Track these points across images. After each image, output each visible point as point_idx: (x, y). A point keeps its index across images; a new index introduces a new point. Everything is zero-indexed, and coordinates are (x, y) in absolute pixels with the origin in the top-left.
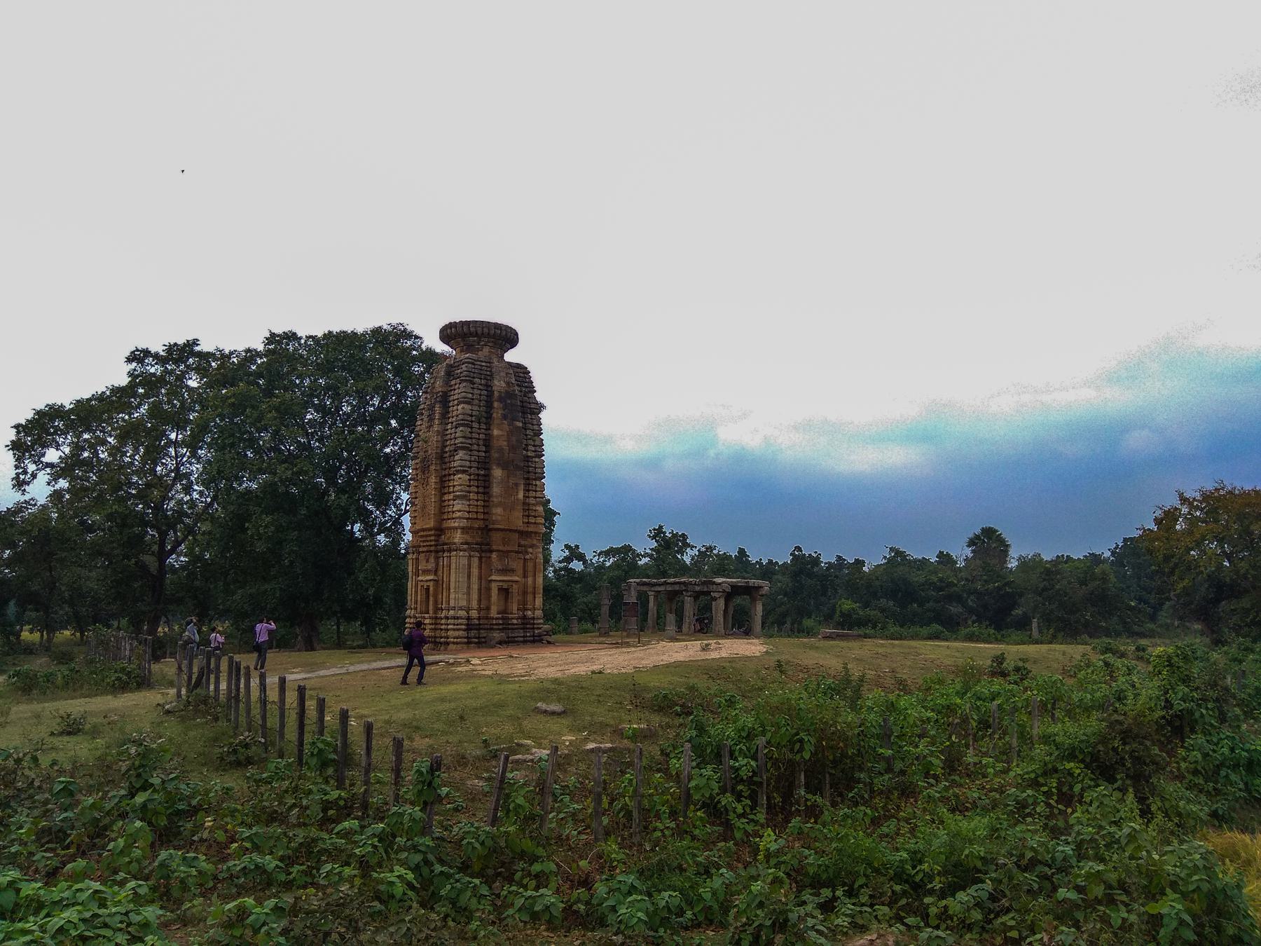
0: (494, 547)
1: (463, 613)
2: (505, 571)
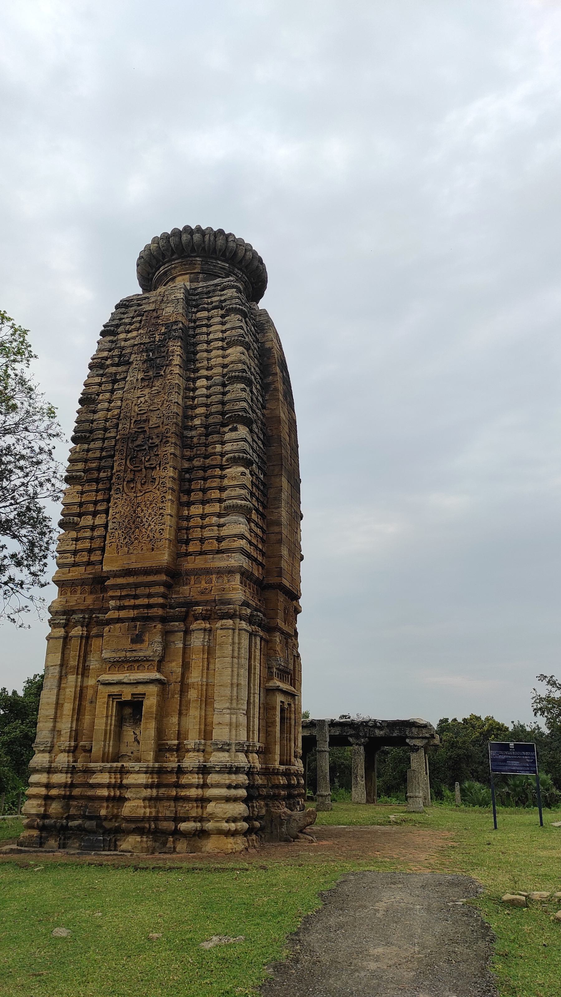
1: (241, 760)
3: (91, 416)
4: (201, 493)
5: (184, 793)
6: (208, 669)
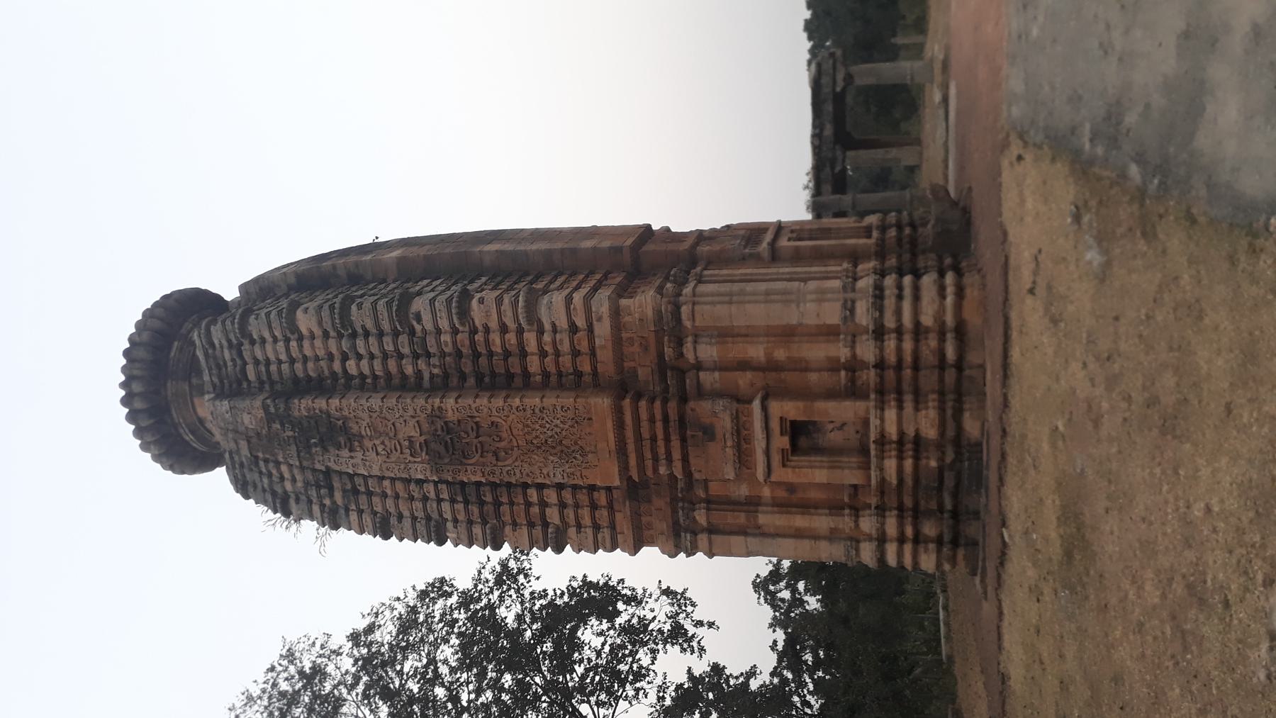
1: (866, 283)
3: (407, 523)
4: (510, 359)
5: (908, 358)
6: (746, 336)
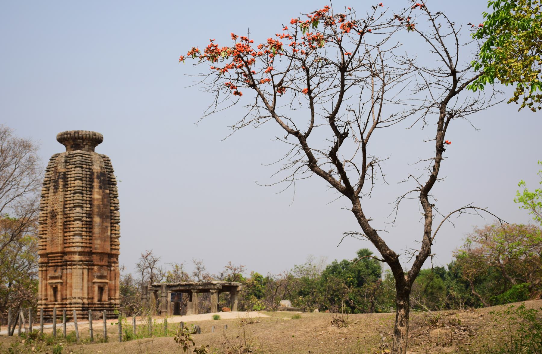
0: (96, 263)
1: (80, 301)
2: (101, 277)
3: (44, 202)
